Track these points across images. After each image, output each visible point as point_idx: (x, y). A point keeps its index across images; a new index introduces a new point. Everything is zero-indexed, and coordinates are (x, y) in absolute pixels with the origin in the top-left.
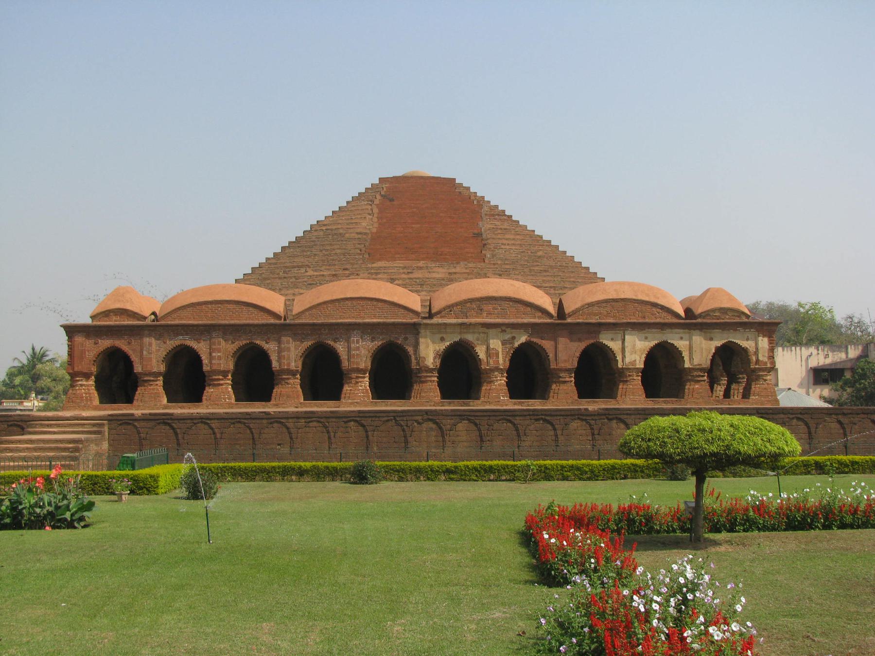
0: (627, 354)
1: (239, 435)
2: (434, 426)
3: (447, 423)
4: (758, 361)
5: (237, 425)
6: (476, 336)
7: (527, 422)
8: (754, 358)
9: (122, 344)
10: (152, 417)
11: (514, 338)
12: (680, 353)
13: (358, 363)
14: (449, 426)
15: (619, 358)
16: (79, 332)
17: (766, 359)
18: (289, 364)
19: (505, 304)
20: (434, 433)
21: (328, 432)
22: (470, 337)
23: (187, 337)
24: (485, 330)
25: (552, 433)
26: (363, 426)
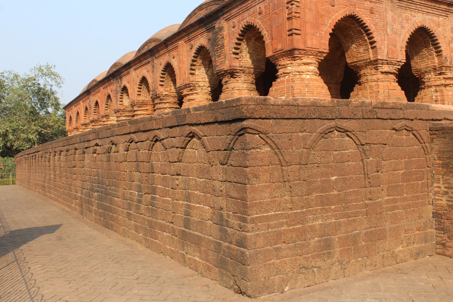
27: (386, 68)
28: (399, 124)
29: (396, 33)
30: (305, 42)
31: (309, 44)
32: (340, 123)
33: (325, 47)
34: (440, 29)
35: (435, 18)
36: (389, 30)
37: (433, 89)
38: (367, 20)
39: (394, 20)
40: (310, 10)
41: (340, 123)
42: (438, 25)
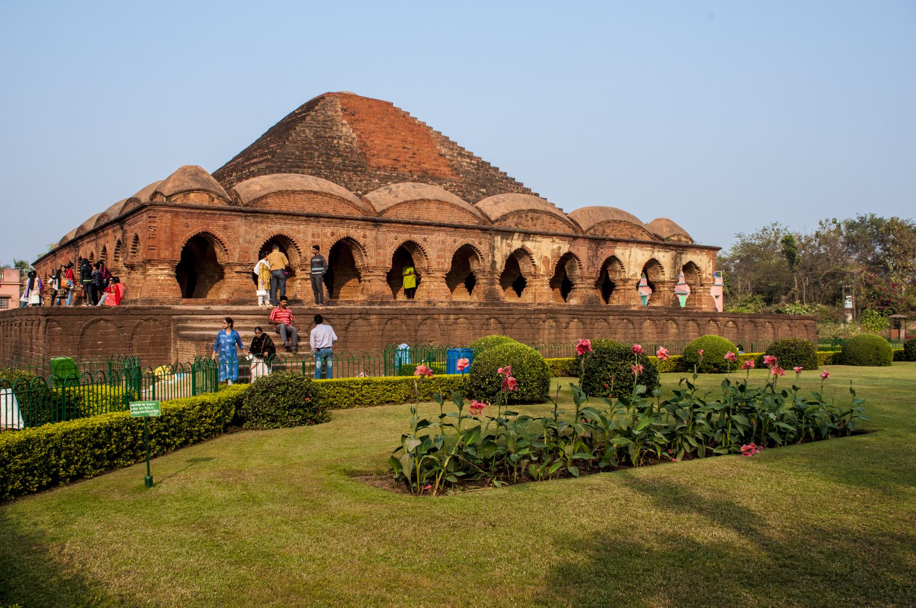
0: (632, 267)
1: (395, 333)
2: (554, 324)
3: (564, 319)
4: (706, 278)
5: (395, 322)
6: (533, 243)
7: (617, 321)
8: (704, 276)
9: (215, 228)
10: (310, 312)
11: (559, 248)
12: (662, 268)
13: (443, 264)
14: (564, 325)
15: (626, 270)
16: (168, 212)
17: (710, 277)
18: (384, 262)
19: (546, 218)
20: (553, 331)
21: (474, 329)
22: (529, 245)
23: (285, 227)
24: (539, 238)
25: (632, 331)
26: (500, 323)
27: (238, 269)
28: (146, 317)
29: (249, 242)
30: (159, 255)
31: (162, 256)
32: (103, 317)
33: (178, 258)
34: (301, 235)
35: (295, 227)
36: (241, 240)
37: (299, 281)
38: (219, 234)
39: (247, 232)
40: (165, 232)
41: (103, 317)
42: (299, 232)
